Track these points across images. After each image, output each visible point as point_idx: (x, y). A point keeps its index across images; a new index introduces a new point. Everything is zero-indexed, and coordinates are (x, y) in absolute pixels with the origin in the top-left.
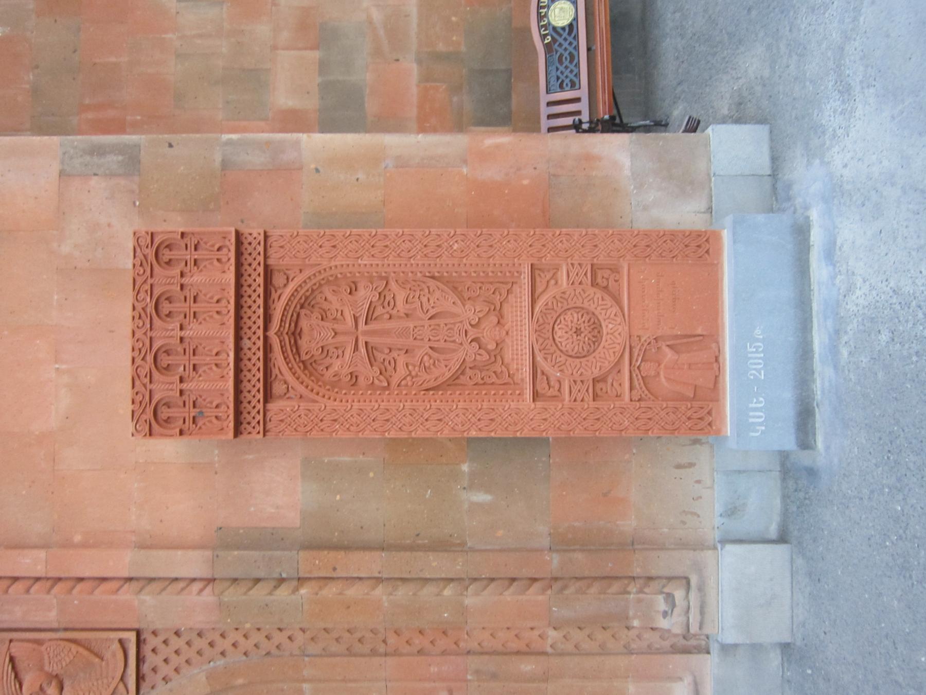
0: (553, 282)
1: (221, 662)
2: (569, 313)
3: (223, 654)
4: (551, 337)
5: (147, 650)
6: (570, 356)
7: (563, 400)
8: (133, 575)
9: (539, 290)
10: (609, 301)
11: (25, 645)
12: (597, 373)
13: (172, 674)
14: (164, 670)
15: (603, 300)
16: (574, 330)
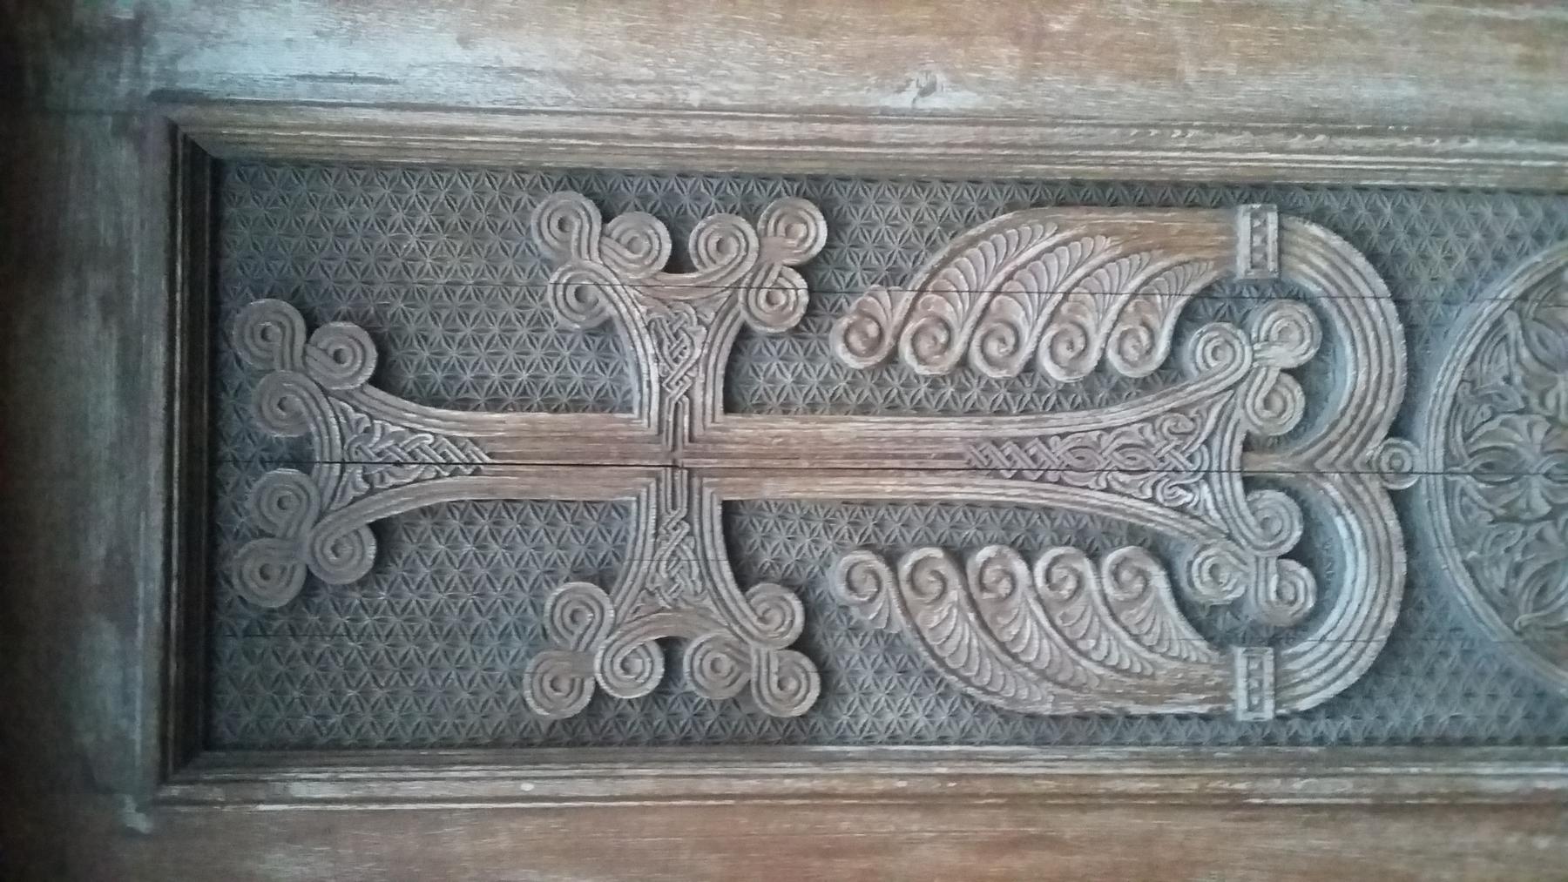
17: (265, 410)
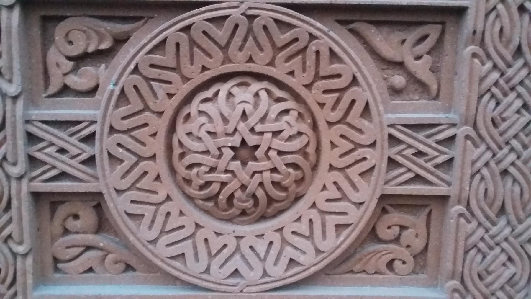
0: (399, 80)
2: (305, 127)
4: (229, 68)
6: (172, 129)
7: (29, 96)
9: (379, 38)
10: (333, 244)
12: (117, 206)
15: (339, 227)
16: (252, 140)
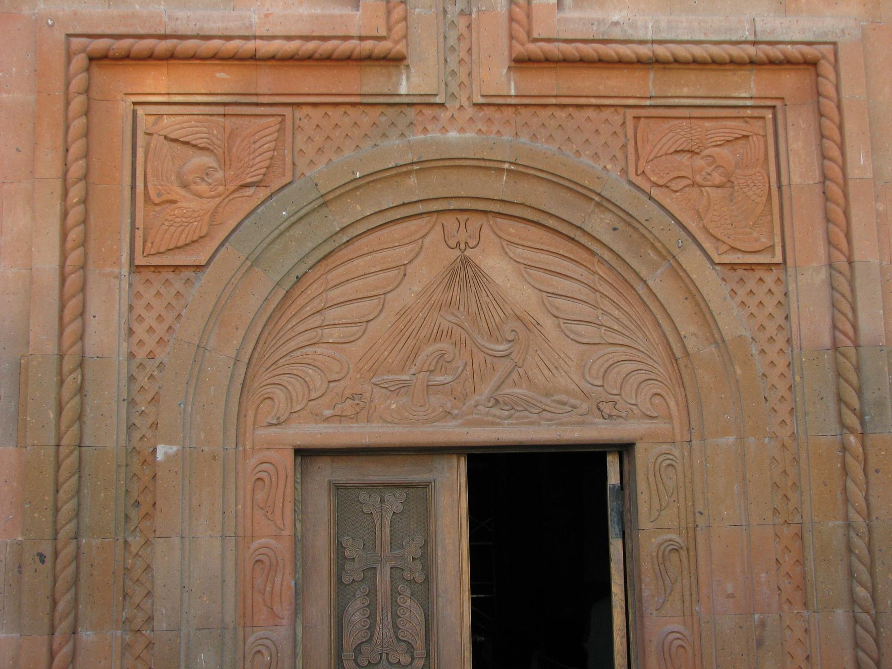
1: (754, 351)
3: (763, 351)
5: (760, 273)
8: (857, 265)
11: (762, 151)
13: (738, 299)
14: (742, 292)
17: (388, 496)
